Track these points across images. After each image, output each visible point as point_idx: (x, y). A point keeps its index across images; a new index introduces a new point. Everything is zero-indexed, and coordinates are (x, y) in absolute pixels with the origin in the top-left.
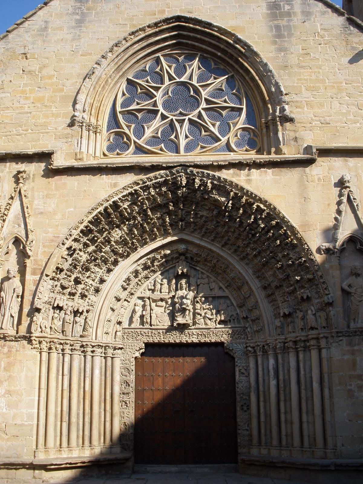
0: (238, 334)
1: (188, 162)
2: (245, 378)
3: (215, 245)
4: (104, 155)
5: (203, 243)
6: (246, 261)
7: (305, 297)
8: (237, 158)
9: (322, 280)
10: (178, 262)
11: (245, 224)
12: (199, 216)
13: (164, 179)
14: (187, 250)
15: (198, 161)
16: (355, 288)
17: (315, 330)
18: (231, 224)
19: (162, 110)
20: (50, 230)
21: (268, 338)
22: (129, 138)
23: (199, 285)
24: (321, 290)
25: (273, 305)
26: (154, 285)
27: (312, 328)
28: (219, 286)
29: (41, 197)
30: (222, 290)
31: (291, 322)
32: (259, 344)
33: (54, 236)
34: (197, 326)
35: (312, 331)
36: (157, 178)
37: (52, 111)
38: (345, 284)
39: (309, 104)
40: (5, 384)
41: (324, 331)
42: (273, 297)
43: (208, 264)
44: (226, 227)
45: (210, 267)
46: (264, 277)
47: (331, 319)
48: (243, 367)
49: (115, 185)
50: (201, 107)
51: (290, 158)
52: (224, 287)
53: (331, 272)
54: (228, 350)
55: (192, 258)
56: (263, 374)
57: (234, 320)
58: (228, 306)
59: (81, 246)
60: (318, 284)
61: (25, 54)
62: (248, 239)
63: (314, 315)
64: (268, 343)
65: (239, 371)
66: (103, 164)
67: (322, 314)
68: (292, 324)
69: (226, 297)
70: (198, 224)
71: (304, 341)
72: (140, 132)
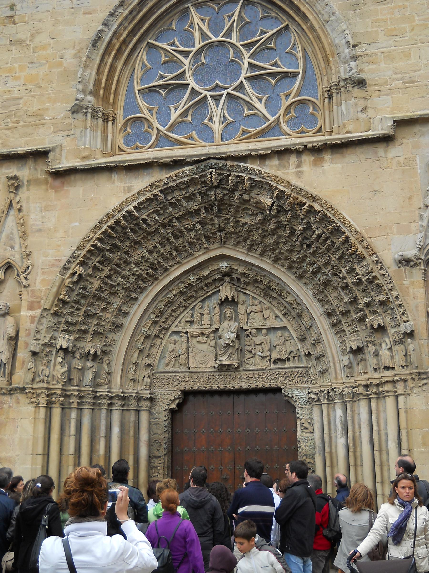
0: (299, 376)
1: (220, 153)
3: (265, 261)
4: (121, 150)
5: (248, 260)
7: (375, 326)
9: (397, 303)
10: (222, 285)
11: (297, 232)
13: (190, 178)
14: (231, 269)
15: (231, 152)
17: (390, 370)
19: (193, 84)
20: (51, 252)
21: (334, 381)
22: (150, 126)
23: (250, 313)
24: (398, 316)
25: (340, 337)
27: (387, 368)
28: (275, 314)
30: (279, 320)
32: (323, 389)
33: (56, 260)
34: (248, 367)
35: (387, 372)
36: (182, 177)
37: (49, 94)
39: (388, 56)
41: (403, 371)
45: (263, 290)
47: (410, 355)
48: (306, 419)
49: (129, 189)
50: (243, 75)
51: (355, 137)
52: (281, 316)
53: (411, 290)
54: (287, 398)
55: (239, 279)
57: (294, 357)
59: (90, 271)
60: (394, 308)
61: (13, 17)
62: (302, 252)
63: (390, 349)
64: (333, 387)
67: (400, 348)
68: (363, 363)
69: (285, 328)
70: (241, 234)
71: (377, 385)
72: (163, 116)
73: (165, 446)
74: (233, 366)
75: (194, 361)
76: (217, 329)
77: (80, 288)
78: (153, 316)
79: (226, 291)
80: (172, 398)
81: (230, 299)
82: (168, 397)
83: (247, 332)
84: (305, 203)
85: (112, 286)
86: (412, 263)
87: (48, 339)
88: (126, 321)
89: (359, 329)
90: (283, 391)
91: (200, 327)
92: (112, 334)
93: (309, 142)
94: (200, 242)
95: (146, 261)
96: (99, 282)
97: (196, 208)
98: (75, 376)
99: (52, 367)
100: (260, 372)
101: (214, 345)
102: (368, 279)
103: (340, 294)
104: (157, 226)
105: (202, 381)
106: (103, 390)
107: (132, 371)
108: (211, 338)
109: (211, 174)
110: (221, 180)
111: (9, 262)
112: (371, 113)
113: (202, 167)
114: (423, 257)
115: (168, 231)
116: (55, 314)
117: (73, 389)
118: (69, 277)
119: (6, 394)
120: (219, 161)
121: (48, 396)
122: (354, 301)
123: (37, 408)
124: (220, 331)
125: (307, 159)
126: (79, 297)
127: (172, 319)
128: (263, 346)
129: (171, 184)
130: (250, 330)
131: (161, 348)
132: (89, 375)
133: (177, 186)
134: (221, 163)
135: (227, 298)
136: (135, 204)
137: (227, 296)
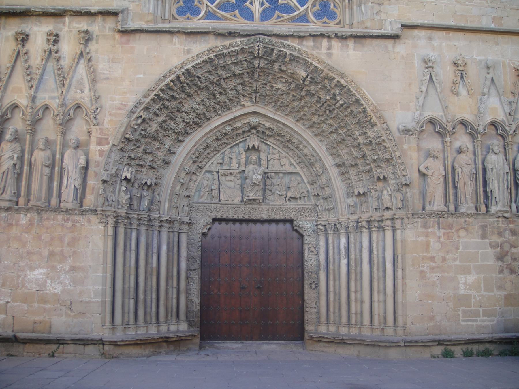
1: (268, 31)
2: (314, 256)
4: (175, 18)
6: (320, 138)
7: (382, 178)
8: (318, 30)
9: (400, 161)
10: (249, 136)
12: (274, 89)
15: (278, 31)
16: (432, 171)
18: (308, 98)
20: (117, 97)
21: (340, 217)
24: (399, 171)
26: (223, 159)
27: (387, 209)
28: (290, 162)
29: (106, 60)
30: (293, 167)
31: (365, 202)
32: (331, 222)
33: (122, 104)
36: (234, 46)
38: (422, 165)
40: (70, 260)
41: (401, 212)
42: (347, 175)
43: (281, 139)
44: (303, 102)
46: (339, 155)
48: (313, 245)
49: (188, 52)
51: (374, 33)
53: (409, 153)
54: (297, 228)
56: (334, 253)
58: (299, 183)
65: (309, 249)
66: (175, 28)
68: (365, 204)
70: (272, 97)
71: (379, 221)
73: (199, 262)
74: (257, 201)
75: (225, 195)
76: (243, 171)
77: (142, 130)
78: (194, 157)
79: (253, 141)
80: (205, 224)
81: (257, 148)
82: (202, 222)
83: (268, 175)
84: (334, 79)
85: (166, 130)
86: (411, 133)
87: (114, 171)
88: (174, 159)
89: (364, 179)
90: (295, 222)
91: (228, 168)
92: (161, 169)
93: (340, 32)
94: (238, 100)
95: (194, 111)
96: (156, 125)
97: (240, 72)
98: (135, 203)
99: (117, 194)
100: (278, 207)
101: (240, 184)
102: (379, 141)
103: (351, 151)
104: (207, 84)
105: (230, 211)
106: (155, 215)
107: (175, 201)
108: (238, 178)
109: (259, 46)
110: (265, 52)
111: (78, 103)
112: (383, 16)
113: (252, 40)
114: (418, 129)
115: (215, 88)
116: (121, 150)
117: (133, 214)
118: (134, 120)
119: (79, 214)
120: (266, 37)
121: (115, 218)
122: (364, 156)
123: (106, 227)
124: (246, 172)
125: (336, 44)
126: (140, 137)
127: (207, 160)
128: (280, 187)
129: (224, 51)
130: (270, 174)
131: (197, 184)
132: (145, 203)
133: (229, 53)
134: (268, 39)
135: (254, 147)
136: (194, 64)
137: (254, 145)
